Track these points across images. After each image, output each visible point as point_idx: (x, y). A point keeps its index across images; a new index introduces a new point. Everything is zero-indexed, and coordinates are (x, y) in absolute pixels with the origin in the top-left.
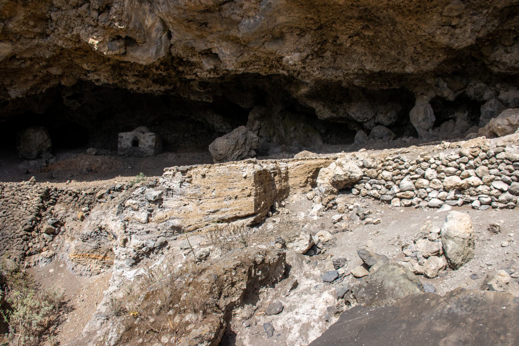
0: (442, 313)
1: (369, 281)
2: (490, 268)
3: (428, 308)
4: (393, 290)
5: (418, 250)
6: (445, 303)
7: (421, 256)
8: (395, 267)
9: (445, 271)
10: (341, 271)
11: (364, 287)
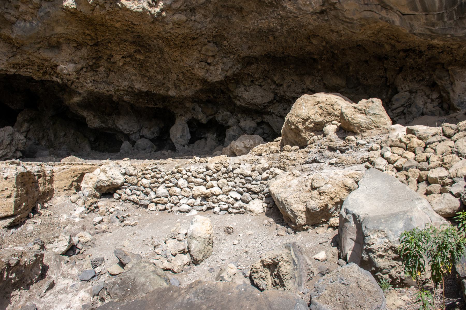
0: (182, 303)
2: (223, 262)
3: (172, 299)
4: (144, 285)
5: (168, 249)
6: (185, 294)
7: (170, 254)
8: (146, 264)
9: (189, 266)
10: (98, 270)
11: (118, 284)
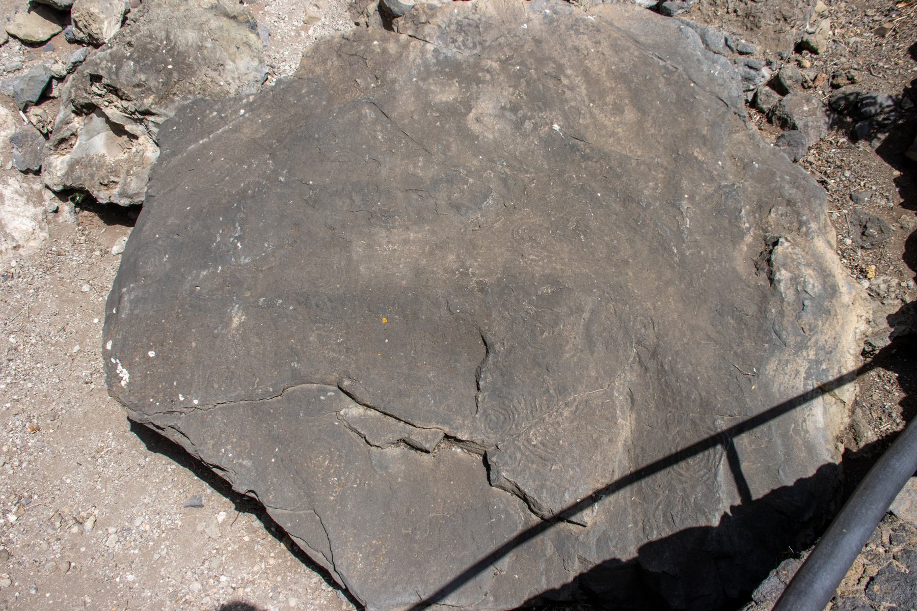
1: (133, 40)
4: (200, 48)
11: (128, 58)
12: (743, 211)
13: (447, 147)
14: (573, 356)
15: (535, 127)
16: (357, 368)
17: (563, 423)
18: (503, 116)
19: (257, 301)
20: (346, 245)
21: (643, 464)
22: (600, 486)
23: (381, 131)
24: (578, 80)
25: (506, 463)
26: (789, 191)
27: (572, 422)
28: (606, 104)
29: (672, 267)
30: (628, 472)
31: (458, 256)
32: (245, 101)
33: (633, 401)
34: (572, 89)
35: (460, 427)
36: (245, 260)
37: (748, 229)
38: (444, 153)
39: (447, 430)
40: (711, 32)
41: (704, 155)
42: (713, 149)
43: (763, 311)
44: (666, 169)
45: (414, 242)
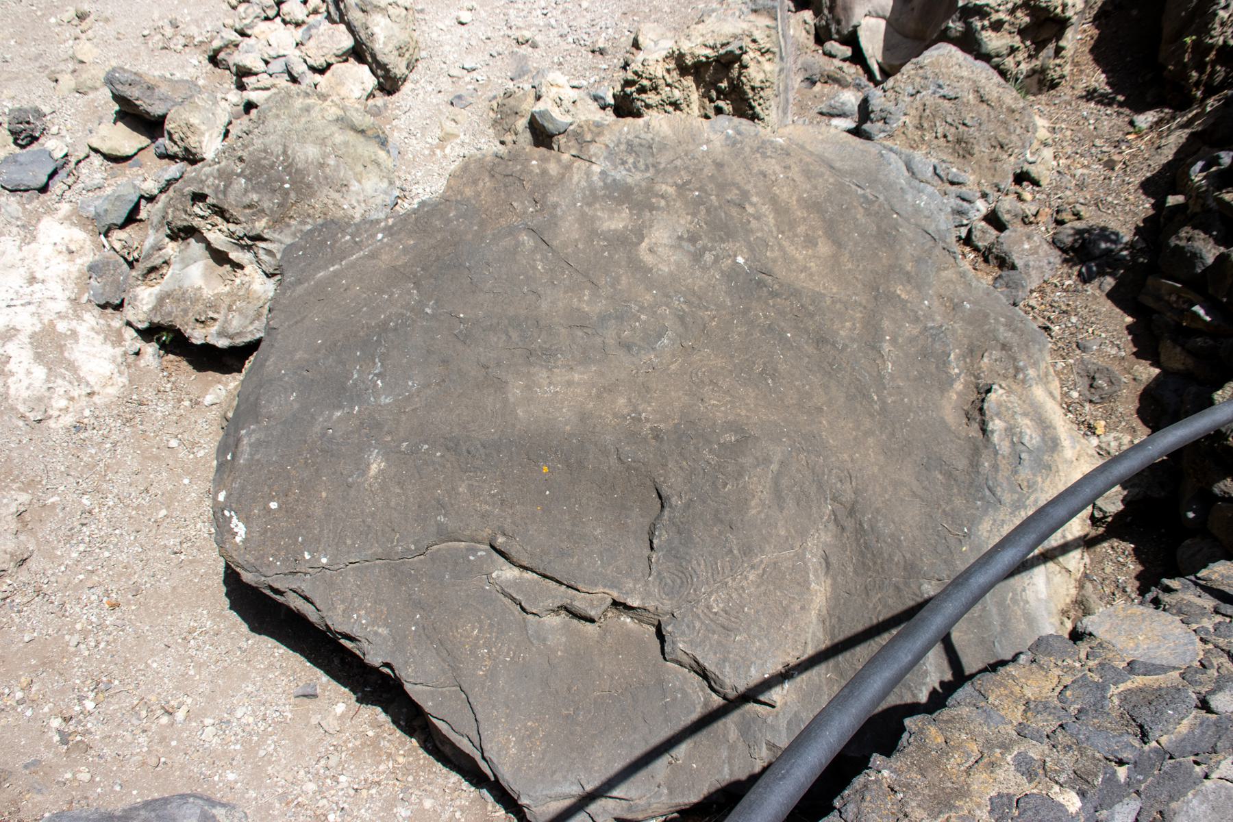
1: (245, 155)
4: (322, 165)
11: (239, 175)
12: (952, 356)
13: (617, 280)
14: (759, 512)
15: (717, 260)
16: (514, 523)
17: (748, 588)
18: (680, 246)
19: (399, 446)
20: (500, 386)
21: (841, 637)
22: (793, 662)
23: (541, 261)
24: (765, 209)
25: (683, 633)
26: (1004, 334)
27: (758, 586)
28: (796, 236)
29: (872, 415)
30: (823, 647)
31: (629, 400)
32: (383, 224)
33: (828, 565)
34: (758, 218)
35: (630, 592)
36: (386, 400)
37: (958, 375)
38: (613, 286)
39: (615, 595)
40: (917, 159)
41: (908, 293)
42: (918, 287)
43: (974, 465)
44: (865, 308)
45: (579, 384)
